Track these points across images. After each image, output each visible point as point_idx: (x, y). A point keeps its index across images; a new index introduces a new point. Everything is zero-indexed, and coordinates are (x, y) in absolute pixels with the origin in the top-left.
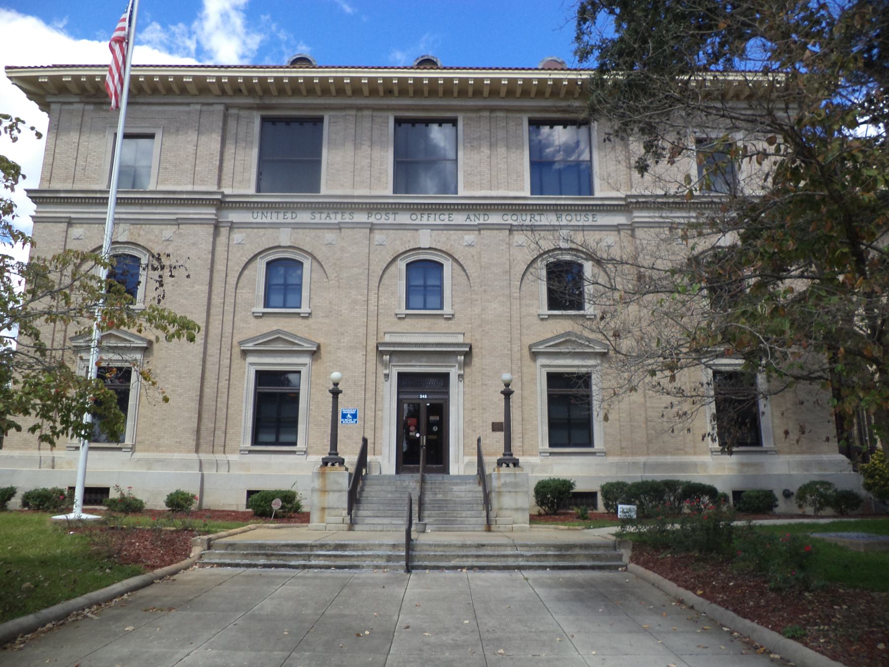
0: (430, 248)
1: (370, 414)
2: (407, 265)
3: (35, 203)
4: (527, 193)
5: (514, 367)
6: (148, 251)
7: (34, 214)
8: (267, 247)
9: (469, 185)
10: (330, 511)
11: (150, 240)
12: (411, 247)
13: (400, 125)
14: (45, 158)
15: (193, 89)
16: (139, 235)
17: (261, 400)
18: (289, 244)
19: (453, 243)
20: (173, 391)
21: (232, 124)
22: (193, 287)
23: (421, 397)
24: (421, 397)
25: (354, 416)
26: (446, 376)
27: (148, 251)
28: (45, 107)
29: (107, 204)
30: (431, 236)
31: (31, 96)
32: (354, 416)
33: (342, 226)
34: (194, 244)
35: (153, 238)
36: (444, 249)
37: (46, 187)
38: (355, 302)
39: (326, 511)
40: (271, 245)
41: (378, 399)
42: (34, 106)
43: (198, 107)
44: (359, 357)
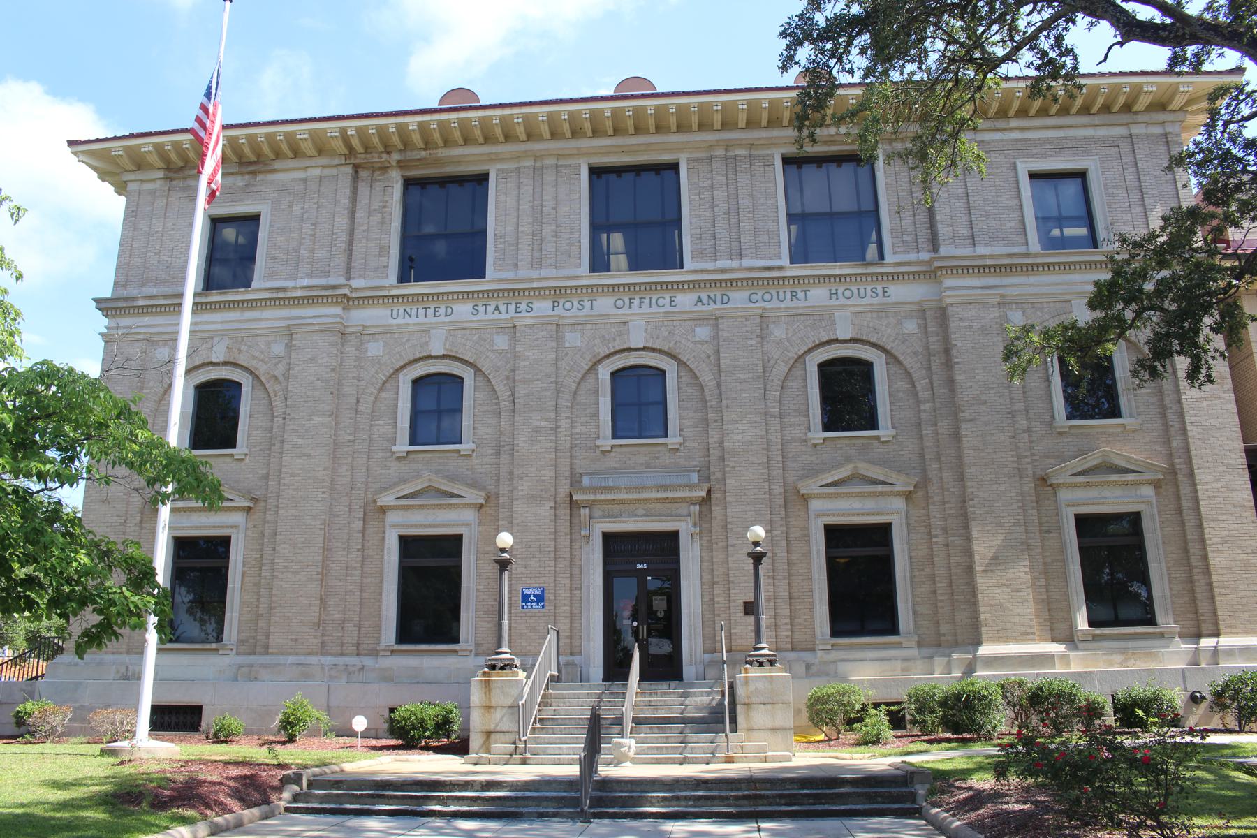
0: (644, 349)
1: (564, 594)
2: (613, 374)
3: (106, 316)
4: (785, 261)
5: (776, 519)
6: (251, 373)
7: (105, 331)
8: (412, 358)
9: (698, 254)
10: (498, 735)
11: (254, 358)
12: (617, 348)
13: (599, 177)
14: (119, 256)
15: (308, 147)
16: (240, 351)
17: (409, 577)
18: (442, 352)
19: (678, 338)
20: (286, 567)
21: (363, 190)
22: (311, 419)
23: (639, 567)
24: (639, 567)
25: (540, 598)
26: (674, 535)
27: (251, 373)
28: (121, 189)
29: (180, 312)
30: (646, 331)
31: (103, 175)
32: (540, 598)
33: (293, 329)
34: (312, 360)
35: (257, 354)
36: (666, 349)
37: (124, 293)
38: (537, 430)
39: (493, 736)
40: (418, 356)
41: (576, 572)
42: (108, 188)
43: (317, 172)
44: (545, 511)
